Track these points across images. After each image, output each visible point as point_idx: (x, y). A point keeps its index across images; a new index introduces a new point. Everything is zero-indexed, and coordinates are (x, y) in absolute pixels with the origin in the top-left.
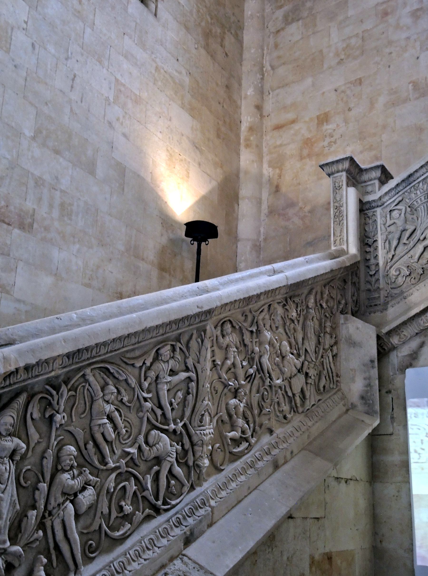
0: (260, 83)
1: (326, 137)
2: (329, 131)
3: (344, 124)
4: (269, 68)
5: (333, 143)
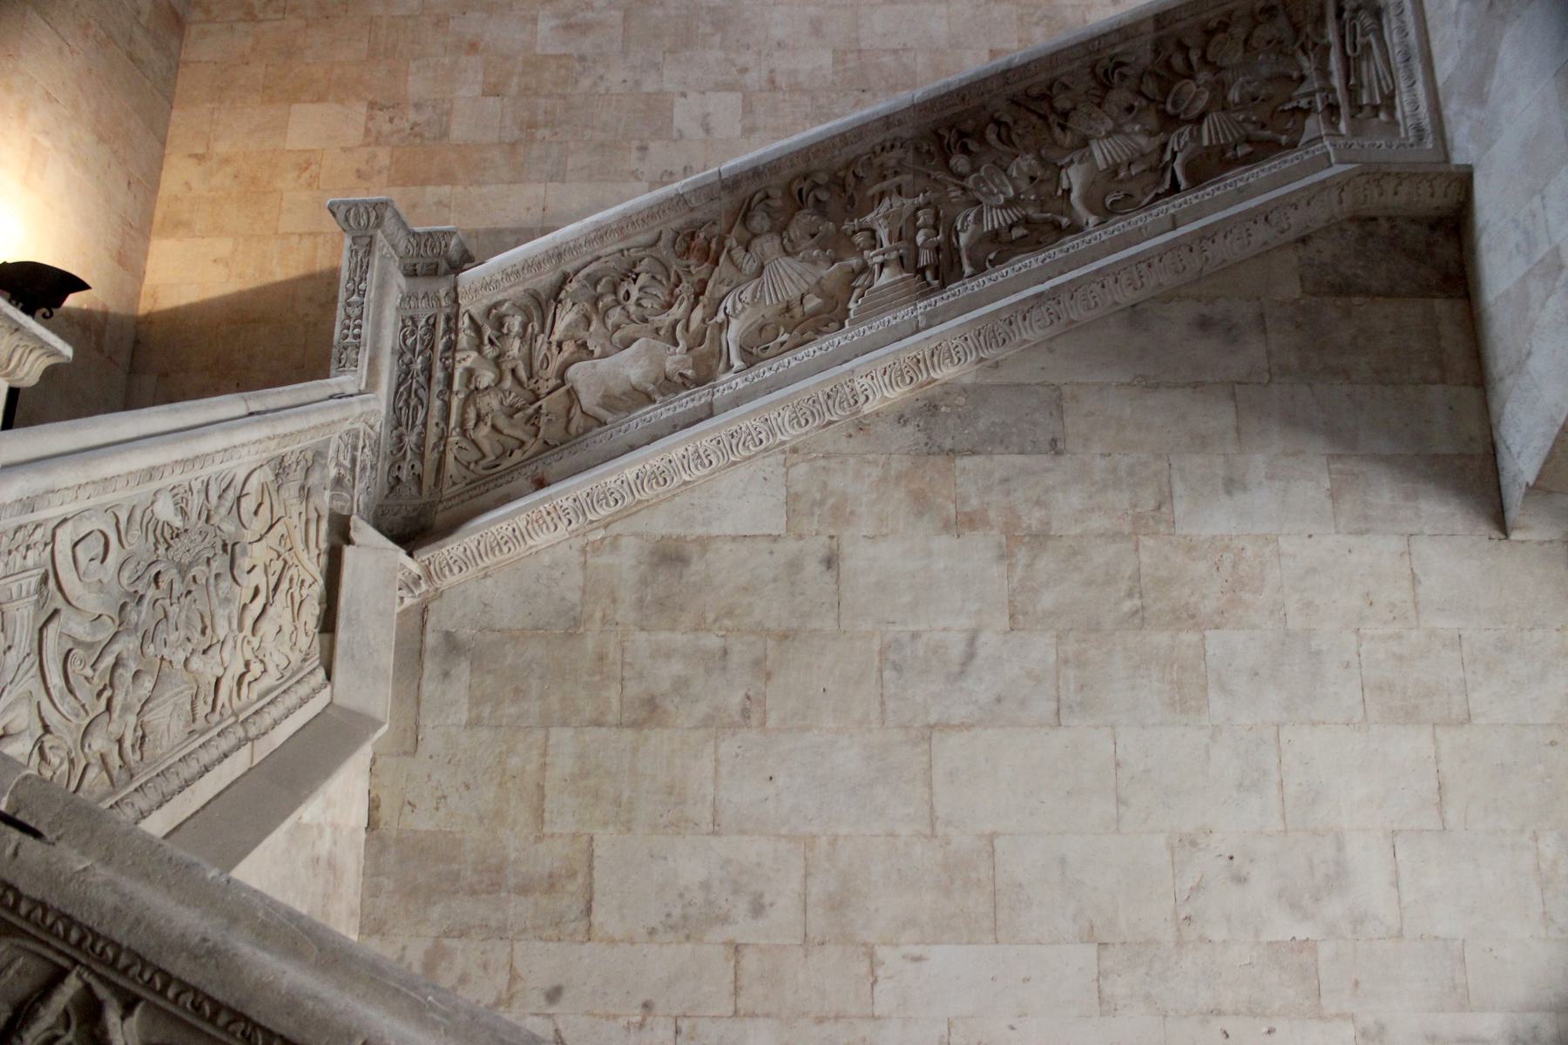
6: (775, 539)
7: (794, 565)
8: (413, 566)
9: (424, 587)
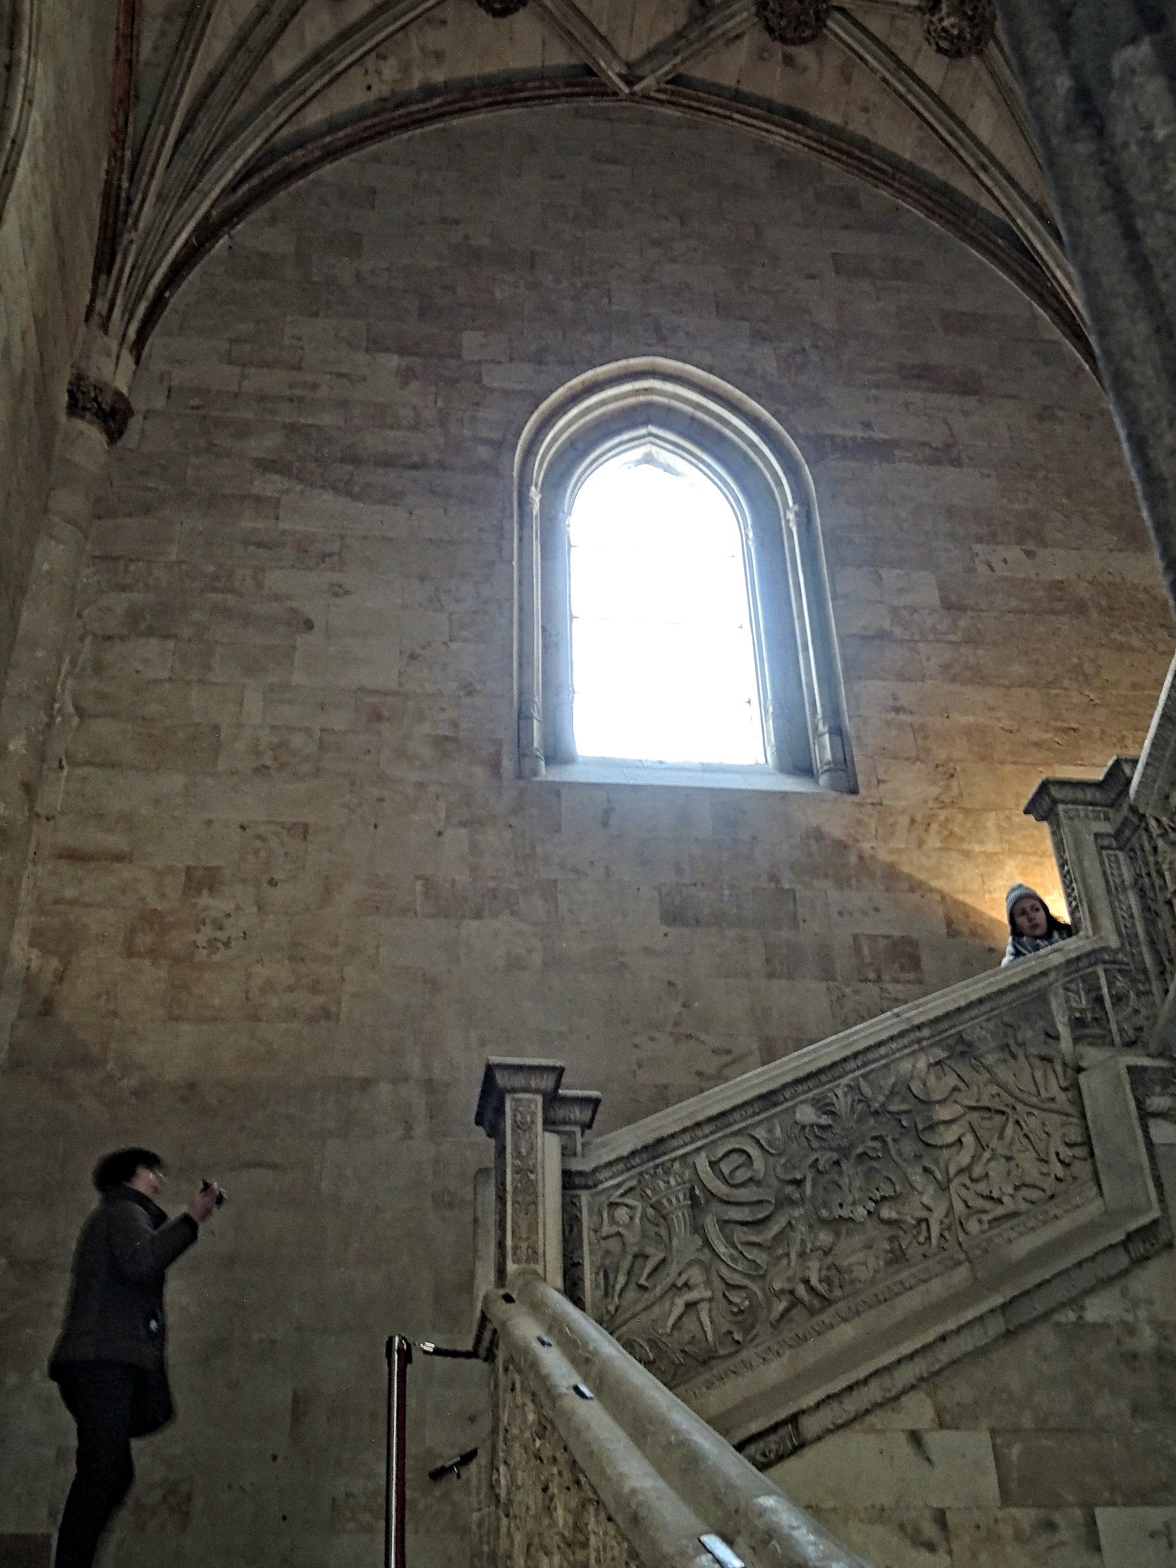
0: (43, 733)
1: (204, 924)
2: (213, 913)
3: (255, 909)
4: (70, 709)
5: (219, 945)
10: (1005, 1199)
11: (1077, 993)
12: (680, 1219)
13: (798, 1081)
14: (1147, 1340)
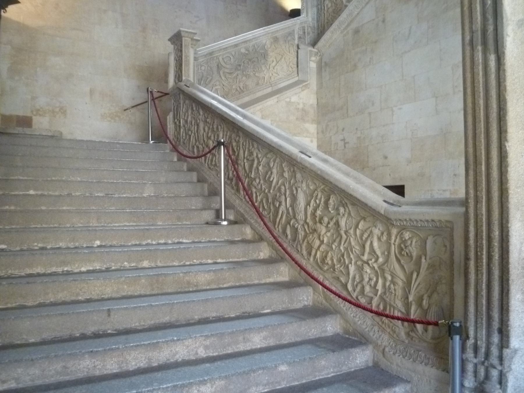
6: (374, 20)
7: (377, 25)
8: (315, 50)
9: (319, 54)
10: (280, 74)
11: (301, 30)
12: (215, 69)
13: (243, 42)
14: (301, 106)
